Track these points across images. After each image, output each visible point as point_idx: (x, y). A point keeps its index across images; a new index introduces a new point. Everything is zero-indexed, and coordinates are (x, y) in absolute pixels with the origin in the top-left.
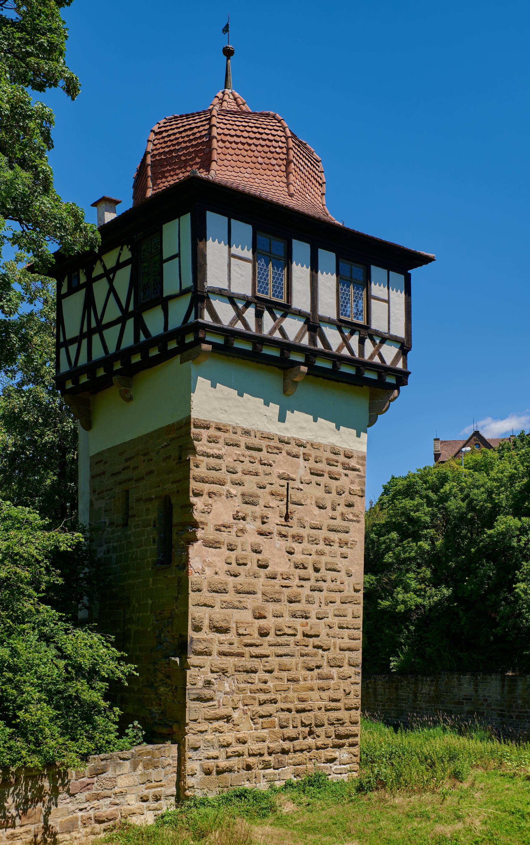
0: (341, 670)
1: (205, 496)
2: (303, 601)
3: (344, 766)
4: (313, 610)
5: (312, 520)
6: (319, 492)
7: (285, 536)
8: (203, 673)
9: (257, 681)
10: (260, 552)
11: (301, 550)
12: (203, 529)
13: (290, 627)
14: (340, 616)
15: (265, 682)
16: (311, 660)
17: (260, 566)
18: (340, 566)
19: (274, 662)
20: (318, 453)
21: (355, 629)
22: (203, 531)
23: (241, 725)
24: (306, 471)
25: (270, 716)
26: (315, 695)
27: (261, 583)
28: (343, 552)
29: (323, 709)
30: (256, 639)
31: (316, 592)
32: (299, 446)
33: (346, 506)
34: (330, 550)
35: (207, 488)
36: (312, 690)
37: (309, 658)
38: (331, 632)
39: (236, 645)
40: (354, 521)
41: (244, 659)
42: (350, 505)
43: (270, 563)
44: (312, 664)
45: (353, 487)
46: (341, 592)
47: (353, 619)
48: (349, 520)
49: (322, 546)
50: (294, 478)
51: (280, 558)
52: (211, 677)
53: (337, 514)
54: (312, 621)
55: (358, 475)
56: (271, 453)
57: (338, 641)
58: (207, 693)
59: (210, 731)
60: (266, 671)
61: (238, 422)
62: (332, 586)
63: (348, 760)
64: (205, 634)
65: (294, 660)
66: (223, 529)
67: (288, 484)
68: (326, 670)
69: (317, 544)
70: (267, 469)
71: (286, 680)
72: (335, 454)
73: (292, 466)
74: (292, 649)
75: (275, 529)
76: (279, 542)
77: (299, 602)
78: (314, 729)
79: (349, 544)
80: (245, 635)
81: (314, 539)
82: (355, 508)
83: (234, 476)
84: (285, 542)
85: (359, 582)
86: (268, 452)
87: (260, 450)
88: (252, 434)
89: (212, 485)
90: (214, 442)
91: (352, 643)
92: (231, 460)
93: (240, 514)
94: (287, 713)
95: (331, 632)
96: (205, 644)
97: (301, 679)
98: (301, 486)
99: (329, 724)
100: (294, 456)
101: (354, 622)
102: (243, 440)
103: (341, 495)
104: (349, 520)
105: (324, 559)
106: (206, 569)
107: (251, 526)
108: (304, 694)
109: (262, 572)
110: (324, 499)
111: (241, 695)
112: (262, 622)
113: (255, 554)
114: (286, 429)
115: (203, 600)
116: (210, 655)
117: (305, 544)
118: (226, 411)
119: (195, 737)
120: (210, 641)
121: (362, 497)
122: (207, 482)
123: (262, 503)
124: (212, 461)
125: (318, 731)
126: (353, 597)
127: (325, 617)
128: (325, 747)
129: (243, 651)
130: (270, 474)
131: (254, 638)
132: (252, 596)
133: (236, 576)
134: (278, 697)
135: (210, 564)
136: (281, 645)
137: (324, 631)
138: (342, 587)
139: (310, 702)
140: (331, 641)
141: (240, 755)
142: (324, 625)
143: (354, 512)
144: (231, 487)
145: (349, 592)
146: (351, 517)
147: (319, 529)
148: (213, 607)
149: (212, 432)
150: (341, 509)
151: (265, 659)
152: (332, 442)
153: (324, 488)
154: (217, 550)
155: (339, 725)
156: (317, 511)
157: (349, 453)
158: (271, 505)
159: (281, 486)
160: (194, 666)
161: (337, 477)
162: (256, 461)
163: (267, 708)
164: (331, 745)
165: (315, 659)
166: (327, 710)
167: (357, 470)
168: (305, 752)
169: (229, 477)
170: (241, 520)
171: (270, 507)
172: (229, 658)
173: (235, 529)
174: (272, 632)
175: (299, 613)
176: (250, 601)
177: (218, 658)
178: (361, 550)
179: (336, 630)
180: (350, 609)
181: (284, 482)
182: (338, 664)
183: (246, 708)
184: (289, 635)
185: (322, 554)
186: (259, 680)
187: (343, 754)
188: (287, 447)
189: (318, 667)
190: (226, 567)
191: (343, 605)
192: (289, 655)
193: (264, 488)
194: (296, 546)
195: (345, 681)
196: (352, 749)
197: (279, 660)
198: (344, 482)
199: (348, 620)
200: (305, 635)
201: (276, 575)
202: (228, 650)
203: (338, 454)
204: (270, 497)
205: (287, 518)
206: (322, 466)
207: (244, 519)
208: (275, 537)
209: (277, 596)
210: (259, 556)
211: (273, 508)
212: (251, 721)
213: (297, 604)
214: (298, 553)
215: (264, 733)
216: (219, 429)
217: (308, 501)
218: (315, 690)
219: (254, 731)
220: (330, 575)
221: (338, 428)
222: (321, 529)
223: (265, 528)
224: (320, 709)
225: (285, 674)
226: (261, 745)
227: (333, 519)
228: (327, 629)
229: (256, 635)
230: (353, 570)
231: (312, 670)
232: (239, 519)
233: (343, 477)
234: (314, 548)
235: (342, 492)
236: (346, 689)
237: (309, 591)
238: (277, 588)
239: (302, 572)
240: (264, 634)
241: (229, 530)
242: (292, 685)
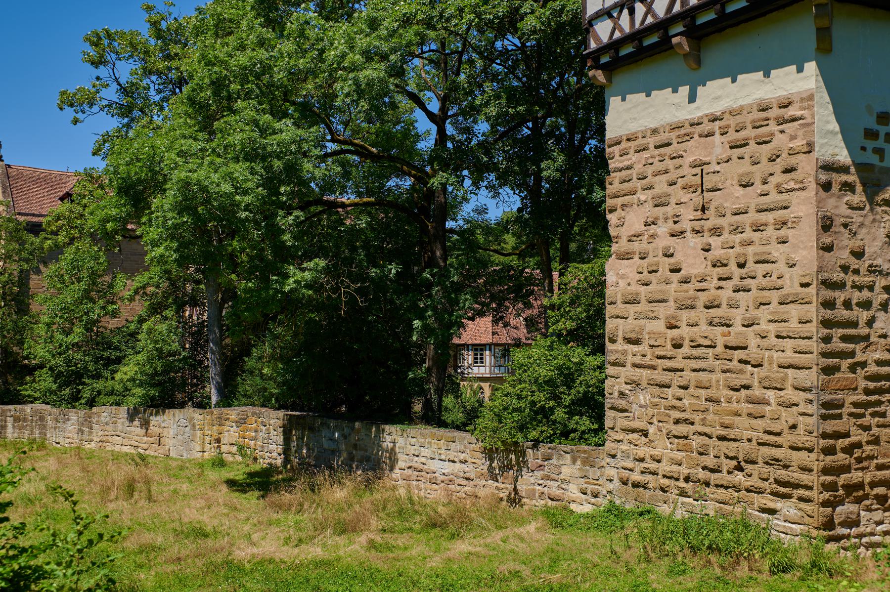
0: (782, 393)
1: (619, 210)
2: (724, 305)
3: (790, 525)
4: (738, 316)
5: (734, 204)
6: (745, 167)
7: (698, 232)
8: (618, 383)
9: (670, 397)
10: (672, 255)
11: (720, 244)
12: (617, 243)
13: (706, 337)
14: (776, 321)
15: (680, 400)
16: (737, 378)
17: (672, 271)
18: (775, 255)
19: (688, 376)
20: (739, 119)
21: (804, 338)
22: (617, 245)
23: (656, 442)
24: (723, 147)
25: (686, 437)
26: (743, 421)
27: (673, 289)
28: (779, 236)
29: (754, 442)
30: (669, 351)
31: (741, 293)
32: (713, 121)
33: (784, 172)
34: (760, 236)
35: (619, 201)
36: (737, 414)
37: (733, 375)
38: (764, 343)
39: (649, 356)
40: (797, 189)
41: (657, 371)
42: (787, 171)
43: (684, 266)
44: (737, 383)
45: (794, 143)
46: (778, 289)
47: (800, 325)
48: (788, 191)
49: (748, 234)
50: (708, 162)
51: (695, 258)
52: (626, 389)
53: (770, 187)
54: (736, 329)
55: (800, 125)
56: (682, 142)
57: (776, 355)
58: (622, 403)
59: (626, 442)
60: (680, 387)
61: (646, 124)
62: (765, 282)
63: (796, 518)
64: (620, 346)
65: (714, 377)
66: (635, 238)
67: (702, 170)
68: (757, 392)
69: (742, 233)
70: (677, 161)
71: (704, 399)
72: (764, 110)
73: (706, 148)
74: (711, 363)
75: (689, 226)
76: (694, 240)
77: (718, 306)
78: (743, 464)
79: (789, 224)
80: (656, 346)
81: (735, 227)
82: (799, 171)
83: (644, 181)
84: (699, 239)
85: (808, 272)
86: (678, 143)
87: (669, 144)
88: (661, 131)
89: (625, 197)
90: (625, 154)
91: (799, 358)
92: (641, 166)
93: (648, 220)
94: (707, 438)
95: (764, 343)
96: (617, 355)
97: (722, 400)
98: (718, 168)
99: (764, 463)
100: (707, 136)
101: (801, 329)
102: (651, 141)
103: (774, 160)
104: (788, 191)
105: (750, 250)
106: (620, 281)
107: (662, 229)
108: (727, 419)
109: (676, 277)
110: (748, 174)
111: (655, 410)
112: (675, 333)
113: (666, 258)
114: (698, 108)
115: (617, 312)
116: (625, 366)
117: (726, 236)
118: (635, 119)
119: (613, 445)
120: (625, 353)
121: (809, 152)
122: (619, 196)
123: (673, 201)
124: (624, 173)
125: (749, 468)
126: (797, 294)
127: (753, 324)
128: (759, 491)
129: (652, 363)
130: (681, 166)
131: (667, 350)
132: (664, 304)
133: (647, 285)
134: (697, 418)
135: (623, 277)
136: (695, 358)
137: (753, 342)
138: (780, 282)
139: (737, 430)
140: (764, 355)
141: (654, 473)
142: (753, 334)
143: (796, 178)
144: (641, 194)
145: (791, 287)
146: (792, 185)
147: (743, 213)
148: (626, 318)
149: (624, 145)
150: (778, 178)
151: (678, 373)
152: (758, 97)
153: (749, 160)
154: (629, 261)
155: (781, 467)
156: (741, 191)
157: (784, 101)
158: (682, 200)
159: (693, 175)
160: (612, 377)
161: (765, 139)
162: (666, 157)
163: (681, 428)
164: (768, 491)
165: (742, 376)
166: (759, 444)
167: (800, 118)
168: (730, 490)
169: (639, 184)
170: (653, 226)
171: (682, 203)
172: (641, 370)
173: (646, 236)
174: (686, 343)
175: (717, 320)
176: (663, 311)
177: (632, 370)
178: (810, 227)
179: (773, 340)
180: (794, 312)
181: (698, 170)
182: (775, 385)
183: (660, 424)
184: (706, 346)
185: (750, 243)
186: (673, 396)
187: (788, 508)
188: (698, 129)
189: (747, 387)
190: (638, 277)
191: (782, 306)
192: (706, 370)
193: (675, 184)
194: (714, 241)
195: (789, 409)
196: (803, 505)
197: (695, 376)
198: (780, 141)
199: (792, 326)
200: (726, 347)
201: (690, 278)
202: (650, 363)
203: (767, 109)
204: (681, 192)
205: (703, 209)
206: (749, 133)
207: (653, 223)
208: (689, 235)
209: (689, 302)
210: (671, 260)
211: (685, 203)
212: (667, 440)
213: (715, 310)
214: (716, 248)
215: (680, 455)
216: (629, 140)
217: (729, 182)
218: (743, 416)
219: (669, 451)
220: (762, 268)
221: (767, 75)
222: (747, 213)
223: (677, 228)
224: (750, 440)
225: (703, 393)
226: (675, 468)
227: (763, 195)
228: (758, 340)
229: (669, 346)
230: (796, 257)
231: (738, 390)
232: (650, 225)
233: (779, 136)
234: (738, 238)
235: (774, 157)
236: (789, 420)
237: (731, 292)
238: (691, 292)
239: (721, 271)
240: (677, 346)
241: (640, 238)
242: (711, 406)
